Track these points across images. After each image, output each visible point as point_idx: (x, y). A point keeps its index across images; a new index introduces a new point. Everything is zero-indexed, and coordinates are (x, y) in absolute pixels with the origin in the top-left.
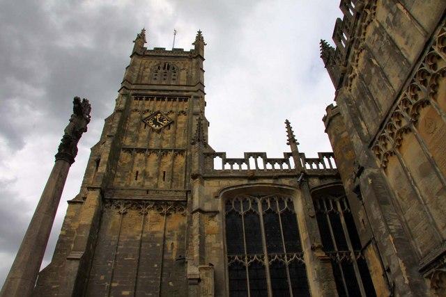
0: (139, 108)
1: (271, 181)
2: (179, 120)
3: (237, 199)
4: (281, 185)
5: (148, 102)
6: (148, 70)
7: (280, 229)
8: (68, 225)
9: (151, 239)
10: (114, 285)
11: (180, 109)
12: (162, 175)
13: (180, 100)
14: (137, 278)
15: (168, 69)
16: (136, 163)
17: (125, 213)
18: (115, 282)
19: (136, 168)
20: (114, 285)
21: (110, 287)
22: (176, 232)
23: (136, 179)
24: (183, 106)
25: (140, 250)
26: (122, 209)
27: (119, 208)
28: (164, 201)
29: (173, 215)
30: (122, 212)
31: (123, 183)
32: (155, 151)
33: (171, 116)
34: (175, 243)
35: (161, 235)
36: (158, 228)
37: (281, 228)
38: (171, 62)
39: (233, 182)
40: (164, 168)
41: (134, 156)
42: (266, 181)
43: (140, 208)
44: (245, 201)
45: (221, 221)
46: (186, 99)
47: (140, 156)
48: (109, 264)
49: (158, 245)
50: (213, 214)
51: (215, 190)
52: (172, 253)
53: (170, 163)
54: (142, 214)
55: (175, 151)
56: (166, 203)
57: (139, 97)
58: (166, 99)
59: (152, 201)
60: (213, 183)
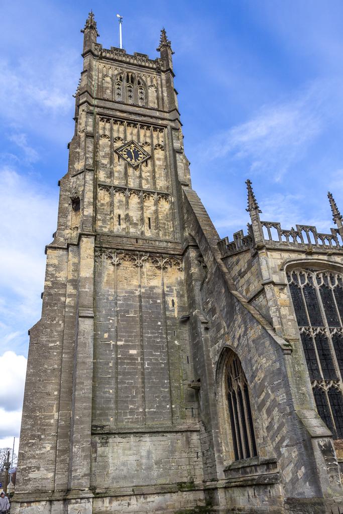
0: (107, 133)
1: (325, 258)
2: (156, 156)
3: (294, 272)
4: (335, 263)
5: (115, 127)
6: (108, 79)
7: (334, 305)
8: (52, 275)
9: (150, 294)
10: (119, 343)
11: (155, 142)
12: (147, 221)
13: (155, 129)
14: (142, 336)
15: (132, 82)
16: (116, 204)
17: (118, 265)
18: (121, 340)
19: (117, 211)
20: (119, 343)
21: (116, 346)
22: (174, 288)
23: (120, 225)
24: (158, 138)
25: (140, 307)
26: (116, 260)
27: (111, 258)
28: (158, 253)
29: (169, 269)
30: (116, 263)
31: (105, 227)
32: (137, 192)
33: (147, 149)
34: (176, 300)
35: (160, 291)
36: (156, 282)
37: (336, 303)
38: (135, 72)
39: (294, 256)
40: (148, 214)
41: (112, 196)
42: (321, 257)
43: (135, 260)
44: (302, 276)
45: (290, 294)
46: (161, 128)
47: (119, 197)
48: (111, 321)
49: (159, 301)
50: (282, 287)
51: (279, 262)
52: (173, 311)
53: (153, 208)
54: (137, 267)
55: (158, 194)
56: (162, 255)
57: (106, 118)
58: (138, 126)
59: (146, 252)
60: (276, 255)
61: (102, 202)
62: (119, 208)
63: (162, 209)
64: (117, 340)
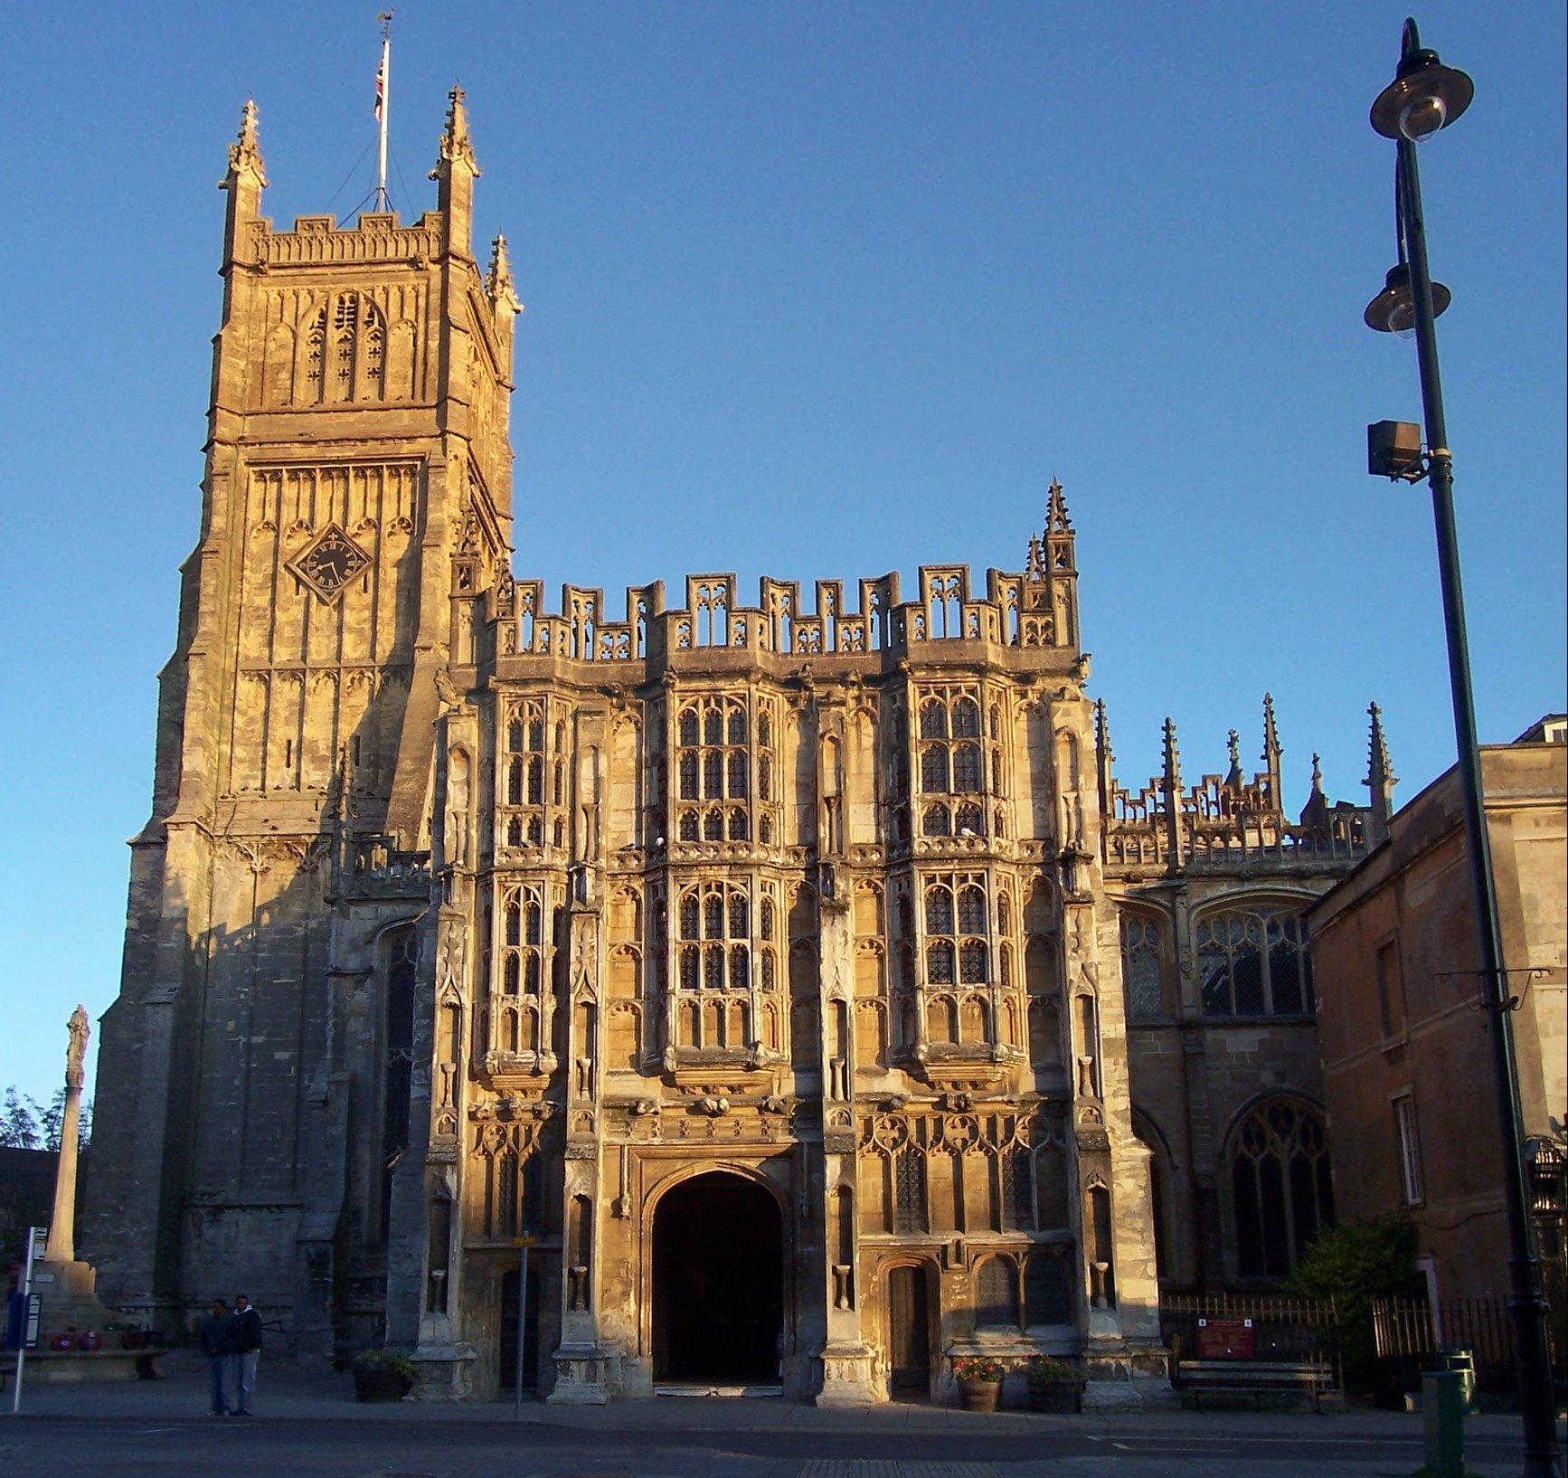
51: (369, 926)
61: (251, 712)
62: (287, 724)
63: (391, 708)
64: (251, 1034)
